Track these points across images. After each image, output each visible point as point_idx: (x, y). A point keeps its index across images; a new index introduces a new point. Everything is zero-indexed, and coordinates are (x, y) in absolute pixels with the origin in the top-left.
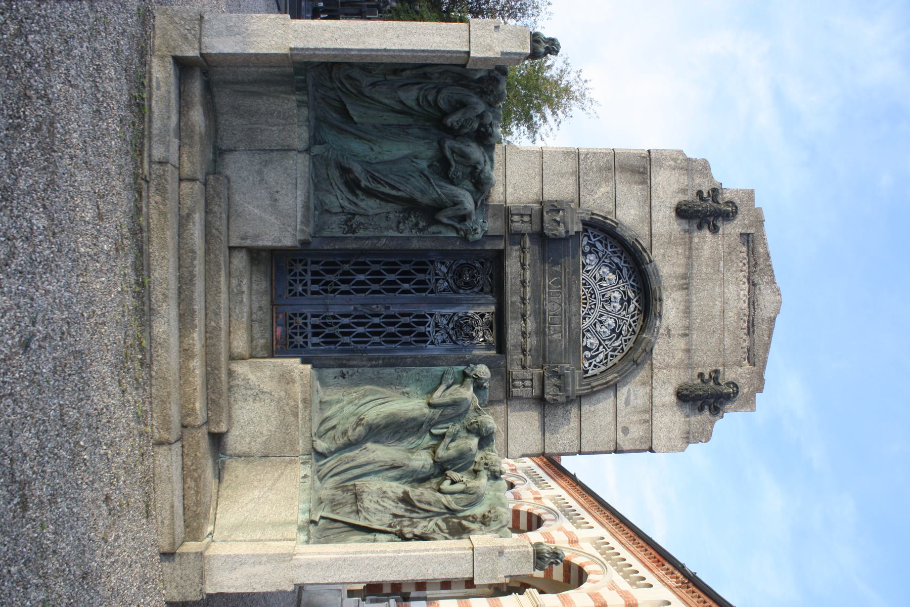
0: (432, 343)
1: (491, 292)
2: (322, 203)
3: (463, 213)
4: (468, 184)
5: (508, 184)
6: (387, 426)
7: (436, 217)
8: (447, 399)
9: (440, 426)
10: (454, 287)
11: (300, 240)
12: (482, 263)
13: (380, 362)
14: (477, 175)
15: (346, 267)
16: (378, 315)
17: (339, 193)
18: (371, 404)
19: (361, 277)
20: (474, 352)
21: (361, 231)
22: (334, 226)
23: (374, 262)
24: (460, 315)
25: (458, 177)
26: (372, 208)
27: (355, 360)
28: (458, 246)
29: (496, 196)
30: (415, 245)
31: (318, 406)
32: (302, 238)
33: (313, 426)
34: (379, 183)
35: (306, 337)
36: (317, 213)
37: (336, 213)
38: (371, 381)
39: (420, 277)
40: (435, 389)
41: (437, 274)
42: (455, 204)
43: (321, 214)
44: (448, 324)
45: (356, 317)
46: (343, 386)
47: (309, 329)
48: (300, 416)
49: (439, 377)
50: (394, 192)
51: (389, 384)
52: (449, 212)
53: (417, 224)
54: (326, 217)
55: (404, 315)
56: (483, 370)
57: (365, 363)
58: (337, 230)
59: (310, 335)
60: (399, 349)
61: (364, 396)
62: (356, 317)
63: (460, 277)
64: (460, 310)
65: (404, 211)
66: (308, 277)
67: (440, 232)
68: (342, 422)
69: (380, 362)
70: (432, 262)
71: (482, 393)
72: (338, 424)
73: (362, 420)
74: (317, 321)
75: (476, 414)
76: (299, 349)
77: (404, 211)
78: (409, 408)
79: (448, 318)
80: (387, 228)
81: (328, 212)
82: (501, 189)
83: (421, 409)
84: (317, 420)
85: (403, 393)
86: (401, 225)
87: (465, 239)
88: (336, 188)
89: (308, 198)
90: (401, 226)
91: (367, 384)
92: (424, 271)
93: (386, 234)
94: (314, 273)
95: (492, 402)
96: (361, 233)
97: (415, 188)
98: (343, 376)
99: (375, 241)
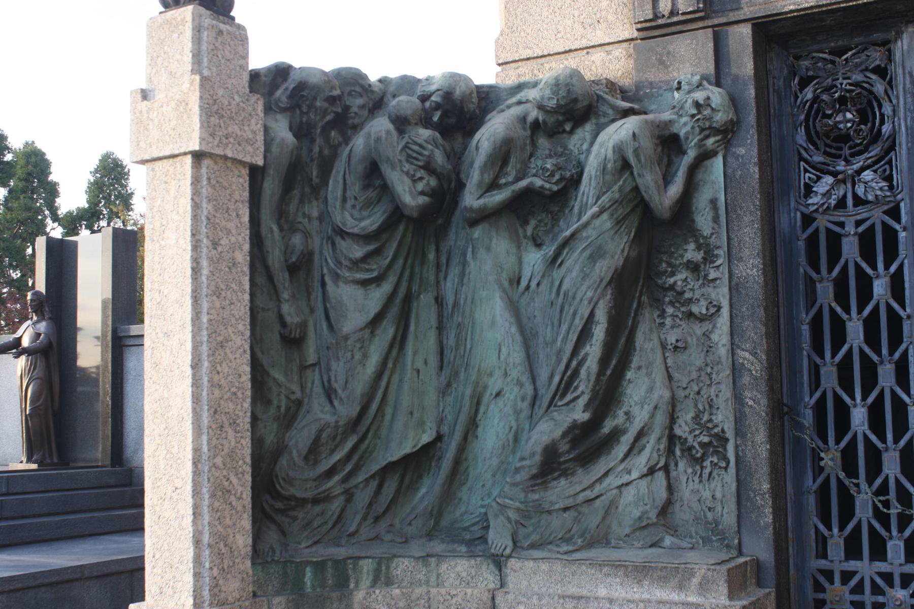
1: (885, 43)
2: (641, 526)
3: (648, 144)
4: (577, 140)
5: (584, 43)
7: (666, 215)
10: (875, 151)
11: (731, 596)
12: (805, 83)
14: (551, 120)
15: (831, 459)
17: (612, 481)
19: (859, 416)
21: (718, 418)
22: (707, 494)
23: (816, 381)
25: (559, 168)
26: (650, 390)
28: (747, 149)
29: (611, 65)
30: (751, 268)
32: (723, 589)
34: (576, 373)
36: (668, 541)
37: (670, 488)
39: (850, 249)
41: (841, 204)
42: (625, 165)
43: (674, 530)
50: (599, 332)
52: (648, 180)
53: (694, 268)
54: (681, 515)
58: (716, 484)
63: (845, 138)
65: (657, 303)
66: (865, 568)
67: (714, 202)
70: (808, 220)
77: (657, 303)
80: (709, 349)
81: (665, 510)
82: (598, 56)
86: (695, 309)
87: (728, 133)
88: (598, 489)
89: (616, 565)
90: (700, 308)
92: (835, 240)
93: (723, 351)
94: (853, 550)
96: (724, 419)
97: (585, 277)
99: (746, 379)
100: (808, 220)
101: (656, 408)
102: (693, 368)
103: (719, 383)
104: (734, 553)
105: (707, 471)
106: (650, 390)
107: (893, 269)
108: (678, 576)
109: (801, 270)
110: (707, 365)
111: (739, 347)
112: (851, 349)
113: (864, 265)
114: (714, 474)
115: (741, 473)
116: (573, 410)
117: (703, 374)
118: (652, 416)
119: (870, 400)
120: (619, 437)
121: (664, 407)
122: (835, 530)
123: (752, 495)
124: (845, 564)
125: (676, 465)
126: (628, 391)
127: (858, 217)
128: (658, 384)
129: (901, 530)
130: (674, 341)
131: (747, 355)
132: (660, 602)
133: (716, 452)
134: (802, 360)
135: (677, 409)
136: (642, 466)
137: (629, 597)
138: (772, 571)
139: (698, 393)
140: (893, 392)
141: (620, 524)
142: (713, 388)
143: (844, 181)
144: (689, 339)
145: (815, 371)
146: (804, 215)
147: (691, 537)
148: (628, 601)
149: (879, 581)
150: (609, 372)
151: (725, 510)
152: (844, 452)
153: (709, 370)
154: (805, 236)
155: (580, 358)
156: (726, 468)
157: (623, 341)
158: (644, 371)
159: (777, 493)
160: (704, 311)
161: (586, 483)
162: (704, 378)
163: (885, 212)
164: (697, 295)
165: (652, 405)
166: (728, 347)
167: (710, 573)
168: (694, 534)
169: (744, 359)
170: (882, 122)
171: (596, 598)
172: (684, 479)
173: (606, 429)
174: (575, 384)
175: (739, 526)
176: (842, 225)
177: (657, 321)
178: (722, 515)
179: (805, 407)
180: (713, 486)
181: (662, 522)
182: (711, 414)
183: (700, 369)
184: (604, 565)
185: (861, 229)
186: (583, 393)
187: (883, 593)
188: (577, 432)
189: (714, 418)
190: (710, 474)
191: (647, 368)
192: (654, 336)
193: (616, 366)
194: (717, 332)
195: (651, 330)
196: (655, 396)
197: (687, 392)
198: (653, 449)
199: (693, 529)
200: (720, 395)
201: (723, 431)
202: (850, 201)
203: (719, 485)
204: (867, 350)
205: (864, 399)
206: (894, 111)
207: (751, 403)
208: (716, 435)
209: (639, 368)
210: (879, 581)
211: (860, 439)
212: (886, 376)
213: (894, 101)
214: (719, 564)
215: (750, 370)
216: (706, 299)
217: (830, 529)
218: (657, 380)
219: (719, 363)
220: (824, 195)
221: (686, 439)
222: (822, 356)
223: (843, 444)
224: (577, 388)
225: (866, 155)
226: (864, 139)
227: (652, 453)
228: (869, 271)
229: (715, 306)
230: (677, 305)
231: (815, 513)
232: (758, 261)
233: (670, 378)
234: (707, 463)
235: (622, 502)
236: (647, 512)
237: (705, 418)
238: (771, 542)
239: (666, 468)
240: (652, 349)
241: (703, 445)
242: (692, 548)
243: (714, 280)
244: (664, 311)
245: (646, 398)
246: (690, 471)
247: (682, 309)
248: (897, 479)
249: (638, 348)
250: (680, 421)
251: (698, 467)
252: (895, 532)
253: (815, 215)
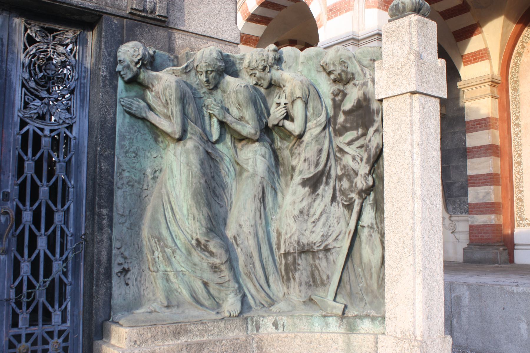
0: (70, 128)
6: (209, 205)
8: (175, 109)
9: (208, 128)
13: (104, 212)
16: (19, 213)
18: (174, 228)
20: (88, 66)
24: (26, 76)
27: (100, 252)
31: (174, 310)
33: (209, 317)
35: (51, 334)
38: (135, 227)
40: (154, 129)
44: (41, 99)
45: (20, 251)
46: (141, 272)
47: (38, 330)
48: (197, 339)
49: (133, 120)
51: (139, 200)
55: (20, 170)
56: (130, 51)
57: (105, 236)
59: (48, 328)
60: (76, 181)
61: (160, 239)
62: (20, 251)
64: (18, 76)
68: (199, 274)
69: (104, 212)
71: (158, 60)
72: (201, 279)
73: (198, 242)
74: (24, 316)
75: (193, 73)
76: (69, 343)
78: (184, 170)
79: (31, 97)
83: (187, 152)
84: (195, 312)
85: (154, 178)
91: (138, 234)
95: (171, 50)
98: (125, 271)
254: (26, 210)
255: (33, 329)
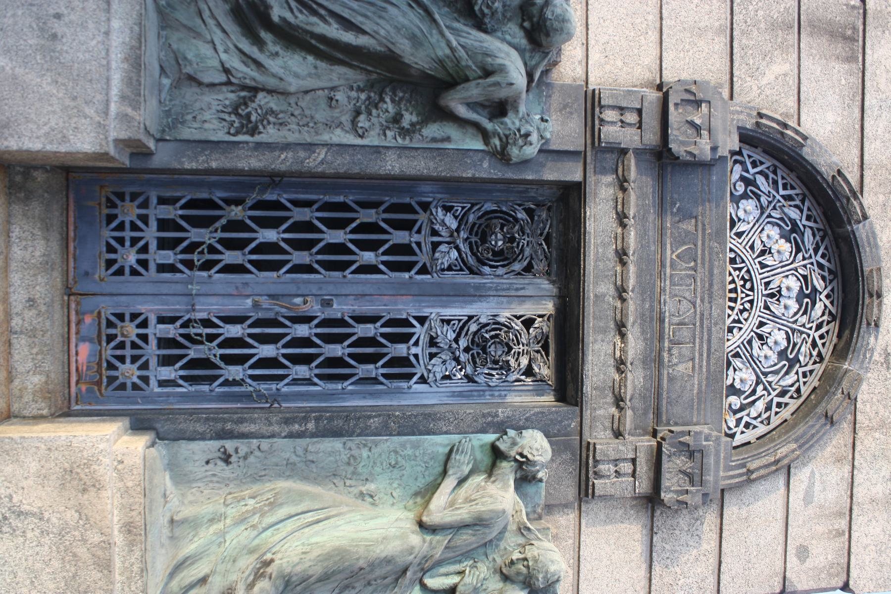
0: (423, 380)
1: (548, 273)
2: (178, 59)
3: (503, 93)
4: (515, 32)
5: (592, 42)
6: (325, 578)
7: (442, 102)
8: (463, 513)
9: (443, 570)
10: (471, 261)
11: (117, 141)
12: (530, 212)
13: (311, 426)
14: (535, 11)
15: (236, 212)
16: (306, 319)
17: (218, 36)
18: (290, 525)
19: (270, 235)
20: (509, 399)
21: (271, 130)
22: (207, 116)
23: (297, 203)
24: (483, 320)
25: (493, 13)
26: (297, 76)
27: (253, 421)
28: (486, 169)
29: (570, 65)
30: (392, 165)
31: (166, 532)
32: (123, 135)
33: (151, 584)
34: (314, 13)
35: (145, 366)
36: (166, 82)
37: (212, 85)
38: (290, 470)
39: (400, 237)
40: (433, 488)
41: (435, 233)
42: (487, 73)
43: (176, 85)
44: (456, 340)
45: (258, 323)
46: (226, 482)
47: (152, 350)
48: (118, 564)
49: (442, 458)
50: (348, 37)
51: (330, 475)
52: (474, 91)
53: (397, 119)
54: (189, 93)
55: (361, 319)
56: (536, 444)
57: (276, 428)
58: (216, 124)
59: (153, 362)
60: (352, 393)
61: (273, 505)
62: (258, 323)
63: (484, 239)
64: (483, 310)
65: (370, 86)
66: (151, 234)
67: (448, 139)
68: (221, 568)
69: (311, 426)
70: (425, 206)
71: (531, 489)
72: (213, 572)
73: (268, 563)
74: (171, 331)
75: (521, 540)
76: (129, 391)
77: (370, 86)
78: (377, 534)
79: (457, 327)
80: (328, 126)
81: (192, 79)
82: (579, 53)
83: (403, 537)
84: (161, 564)
85: (362, 495)
86: (362, 118)
87: (502, 156)
88: (211, 22)
89: (140, 38)
90: (363, 121)
91: (280, 475)
92: (407, 226)
93: (326, 137)
94: (163, 225)
95: (549, 508)
96: (270, 134)
97: (398, 29)
98: (226, 458)
99: (302, 154)
100: (425, 206)
101: (281, 79)
102: (313, 112)
103: (300, 132)
104: (158, 136)
105: (227, 117)
106: (297, 76)
107: (382, 267)
108: (133, 95)
109: (387, 198)
110: (315, 123)
111: (329, 150)
112: (323, 232)
113: (386, 246)
114: (224, 123)
115: (225, 145)
116: (282, 7)
117: (308, 119)
118: (274, 76)
119: (283, 244)
120: (257, 45)
121: (281, 86)
122: (180, 212)
123: (206, 153)
124: (154, 218)
125: (232, 92)
126: (296, 57)
127: (423, 244)
128: (301, 82)
129: (183, 262)
130: (337, 97)
131: (322, 156)
132: (108, 80)
133: (242, 126)
134: (316, 194)
135: (280, 96)
136: (231, 63)
137: (113, 49)
138: (144, 166)
139: (292, 115)
140: (288, 261)
141: (180, 40)
142: (296, 127)
143: (451, 236)
144: (338, 110)
145: (308, 204)
146: (429, 203)
147: (171, 100)
148: (108, 50)
149: (142, 243)
150: (313, 42)
151: (193, 130)
152: (242, 222)
153: (311, 125)
154: (413, 203)
155: (327, 18)
156: (229, 133)
157: (340, 56)
158: (313, 71)
159: (209, 172)
160: (360, 125)
161: (216, 12)
162: (305, 120)
163: (425, 264)
164: (374, 120)
165: (283, 76)
166: (329, 142)
167: (136, 124)
168: (173, 103)
169: (319, 154)
170: (491, 267)
171: (109, 20)
172: (220, 97)
173: (263, 34)
174: (305, 11)
175: (180, 140)
176: (419, 232)
177: (355, 85)
178: (189, 128)
179: (279, 195)
180: (215, 121)
181: (182, 77)
182: (274, 124)
183: (312, 117)
184: (140, 28)
185: (414, 246)
186: (296, 17)
187: (132, 245)
188: (262, 8)
189: (271, 126)
190: (224, 120)
191: (315, 74)
192: (342, 82)
193: (318, 48)
194: (342, 134)
195: (347, 79)
196: (291, 79)
197: (294, 105)
198: (245, 74)
199: (177, 102)
200: (290, 133)
201: (260, 133)
202: (436, 239)
203: (215, 127)
204: (321, 244)
205: (284, 240)
206: (498, 276)
207: (283, 156)
208: (256, 127)
209: (316, 67)
210: (142, 243)
211: (253, 235)
212: (300, 257)
213: (505, 276)
214: (146, 129)
215: (309, 158)
216: (370, 127)
217: (182, 208)
218: (305, 82)
219: (317, 133)
220: (443, 221)
221: (254, 101)
222: (318, 210)
223: (248, 222)
224: (301, 12)
225: (469, 253)
226: (481, 254)
227: (242, 72)
228: (381, 250)
229: (364, 133)
230: (367, 102)
231: (194, 197)
232: (397, 171)
233: (306, 92)
234: (233, 118)
235: (200, 43)
236: (191, 64)
237: (271, 119)
238: (168, 167)
239: (229, 83)
240: (331, 80)
241: (249, 115)
242: (160, 102)
243: (385, 135)
244: (362, 91)
245: (290, 71)
246: (227, 102)
247: (363, 107)
248: (221, 261)
249: (333, 67)
250: (269, 98)
251: (230, 110)
252: (180, 257)
253: (428, 212)
254: (310, 328)
255: (153, 342)
